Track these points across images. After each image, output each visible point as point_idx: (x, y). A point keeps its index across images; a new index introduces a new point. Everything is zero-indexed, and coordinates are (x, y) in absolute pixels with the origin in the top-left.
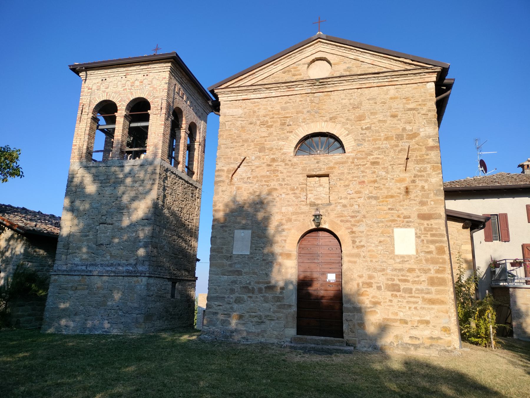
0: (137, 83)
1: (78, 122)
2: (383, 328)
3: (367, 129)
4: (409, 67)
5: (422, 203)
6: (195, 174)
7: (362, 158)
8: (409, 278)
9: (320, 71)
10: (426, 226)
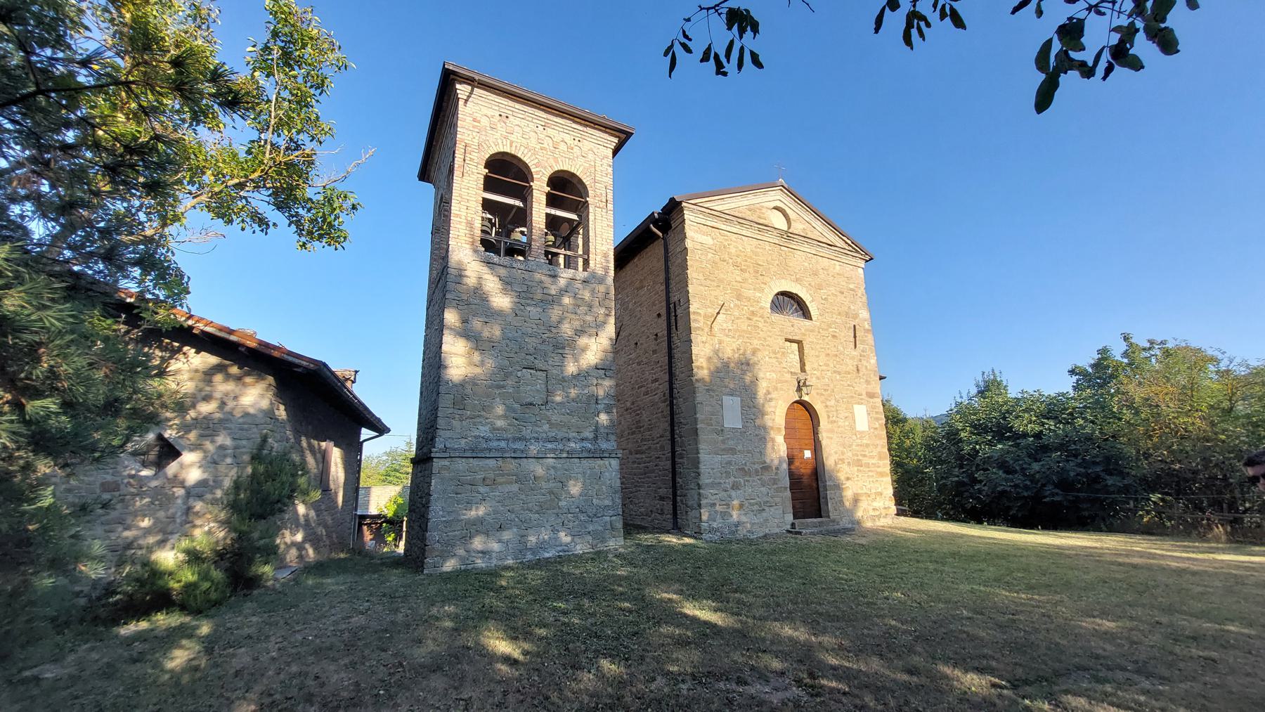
0: (563, 147)
2: (856, 501)
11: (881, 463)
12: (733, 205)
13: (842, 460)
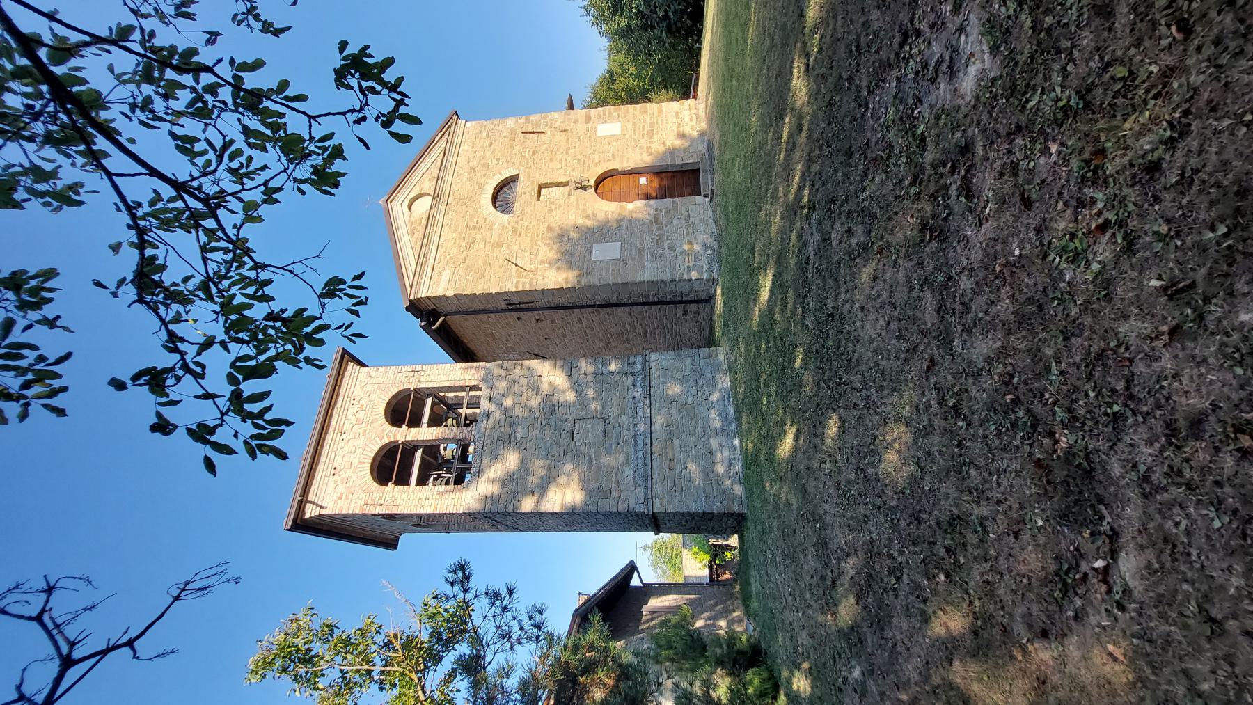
0: (361, 415)
11: (650, 111)
12: (410, 250)
13: (648, 148)
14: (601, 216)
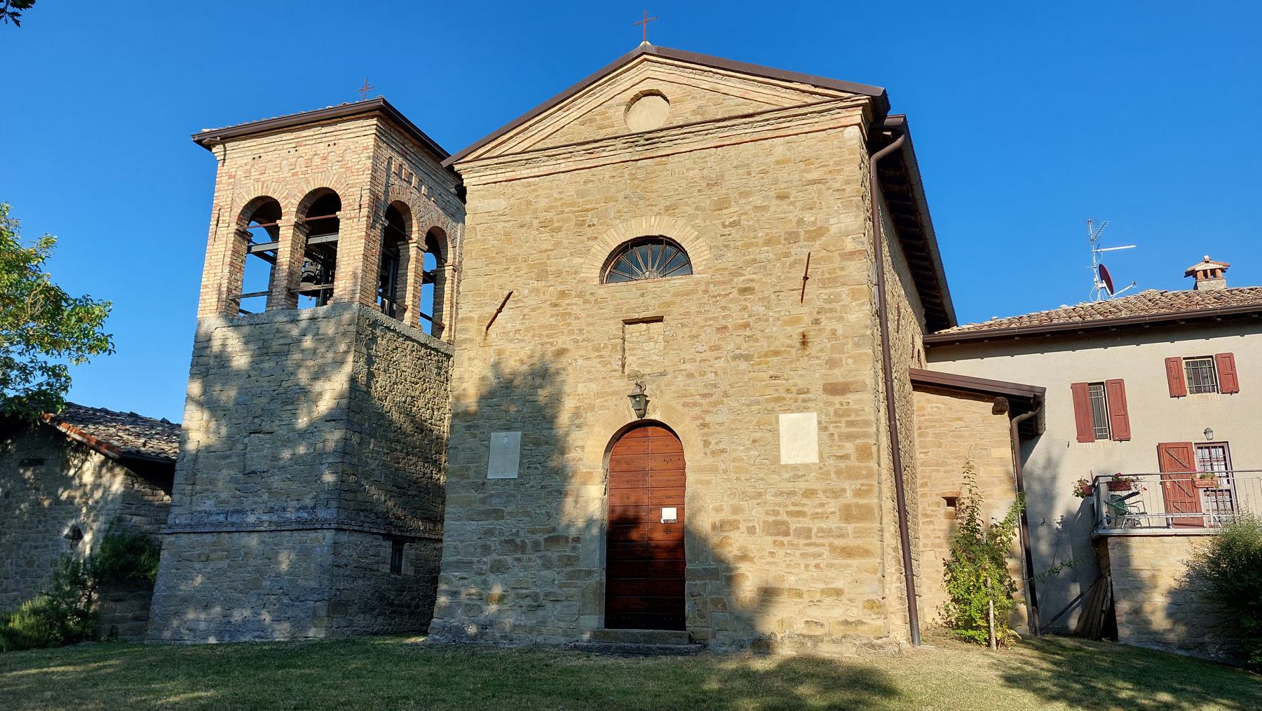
0: (317, 160)
1: (210, 241)
3: (732, 225)
4: (810, 100)
5: (832, 363)
6: (446, 329)
7: (724, 283)
8: (805, 509)
9: (648, 116)
10: (838, 406)
14: (576, 438)
